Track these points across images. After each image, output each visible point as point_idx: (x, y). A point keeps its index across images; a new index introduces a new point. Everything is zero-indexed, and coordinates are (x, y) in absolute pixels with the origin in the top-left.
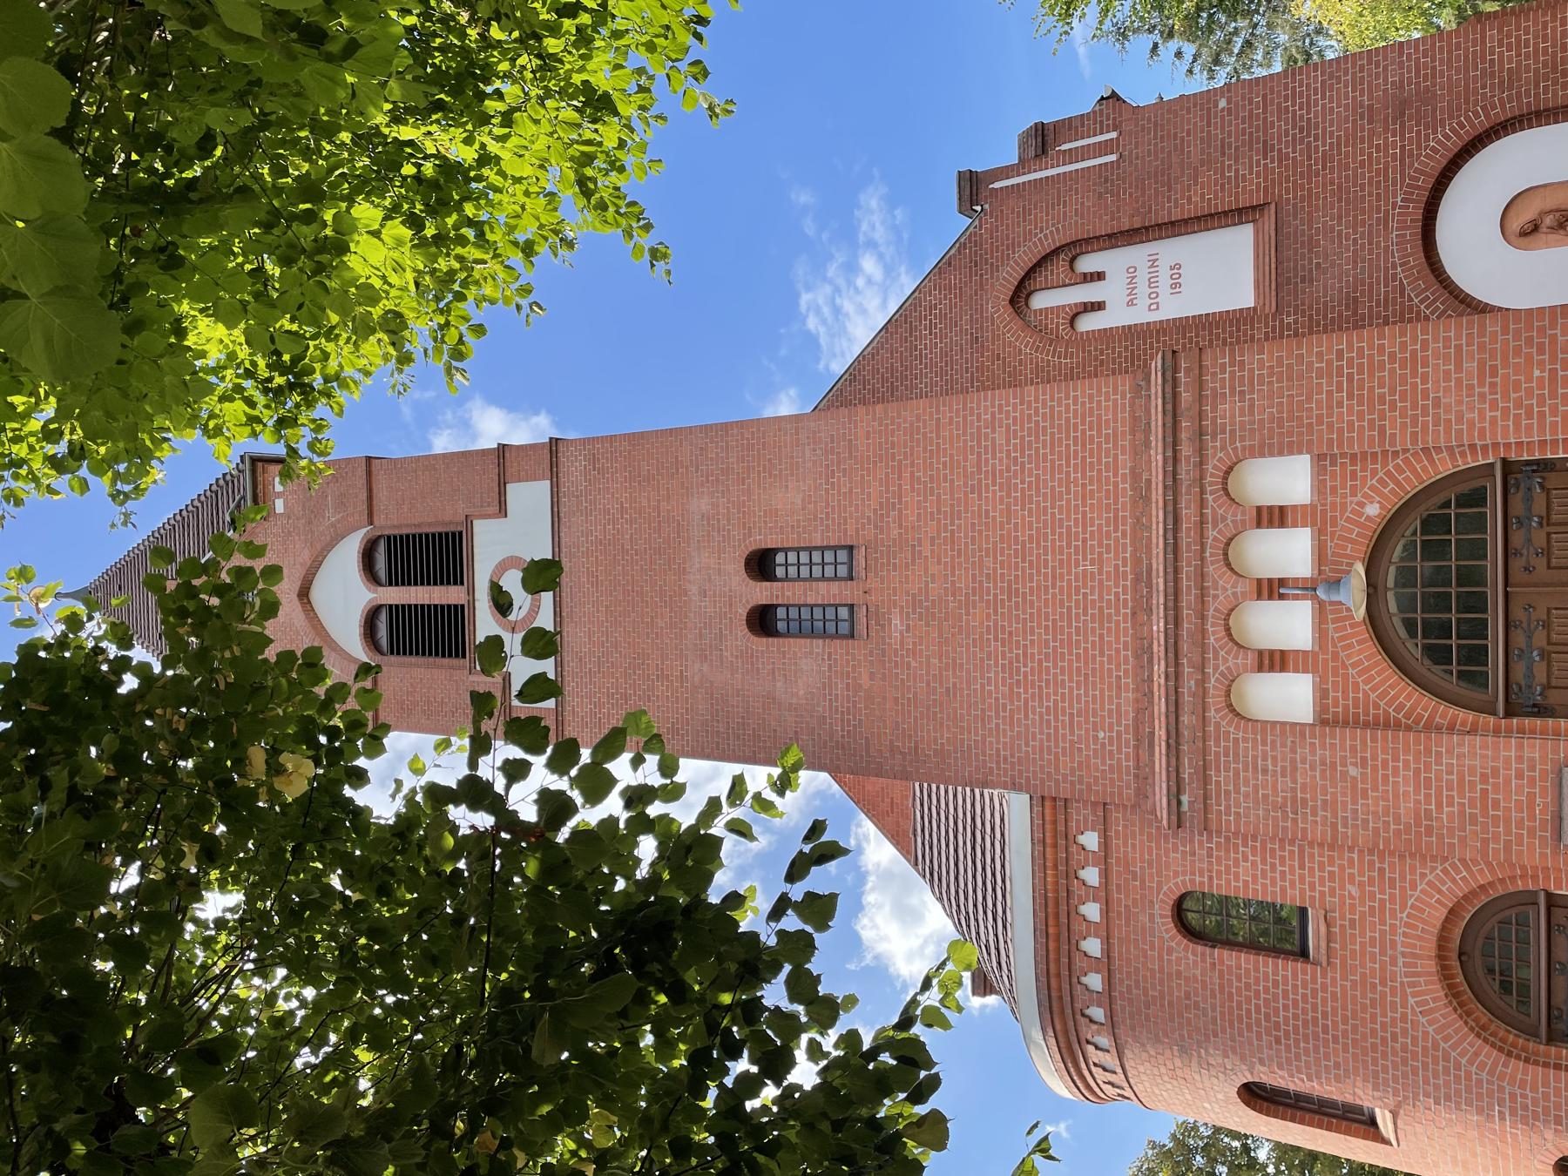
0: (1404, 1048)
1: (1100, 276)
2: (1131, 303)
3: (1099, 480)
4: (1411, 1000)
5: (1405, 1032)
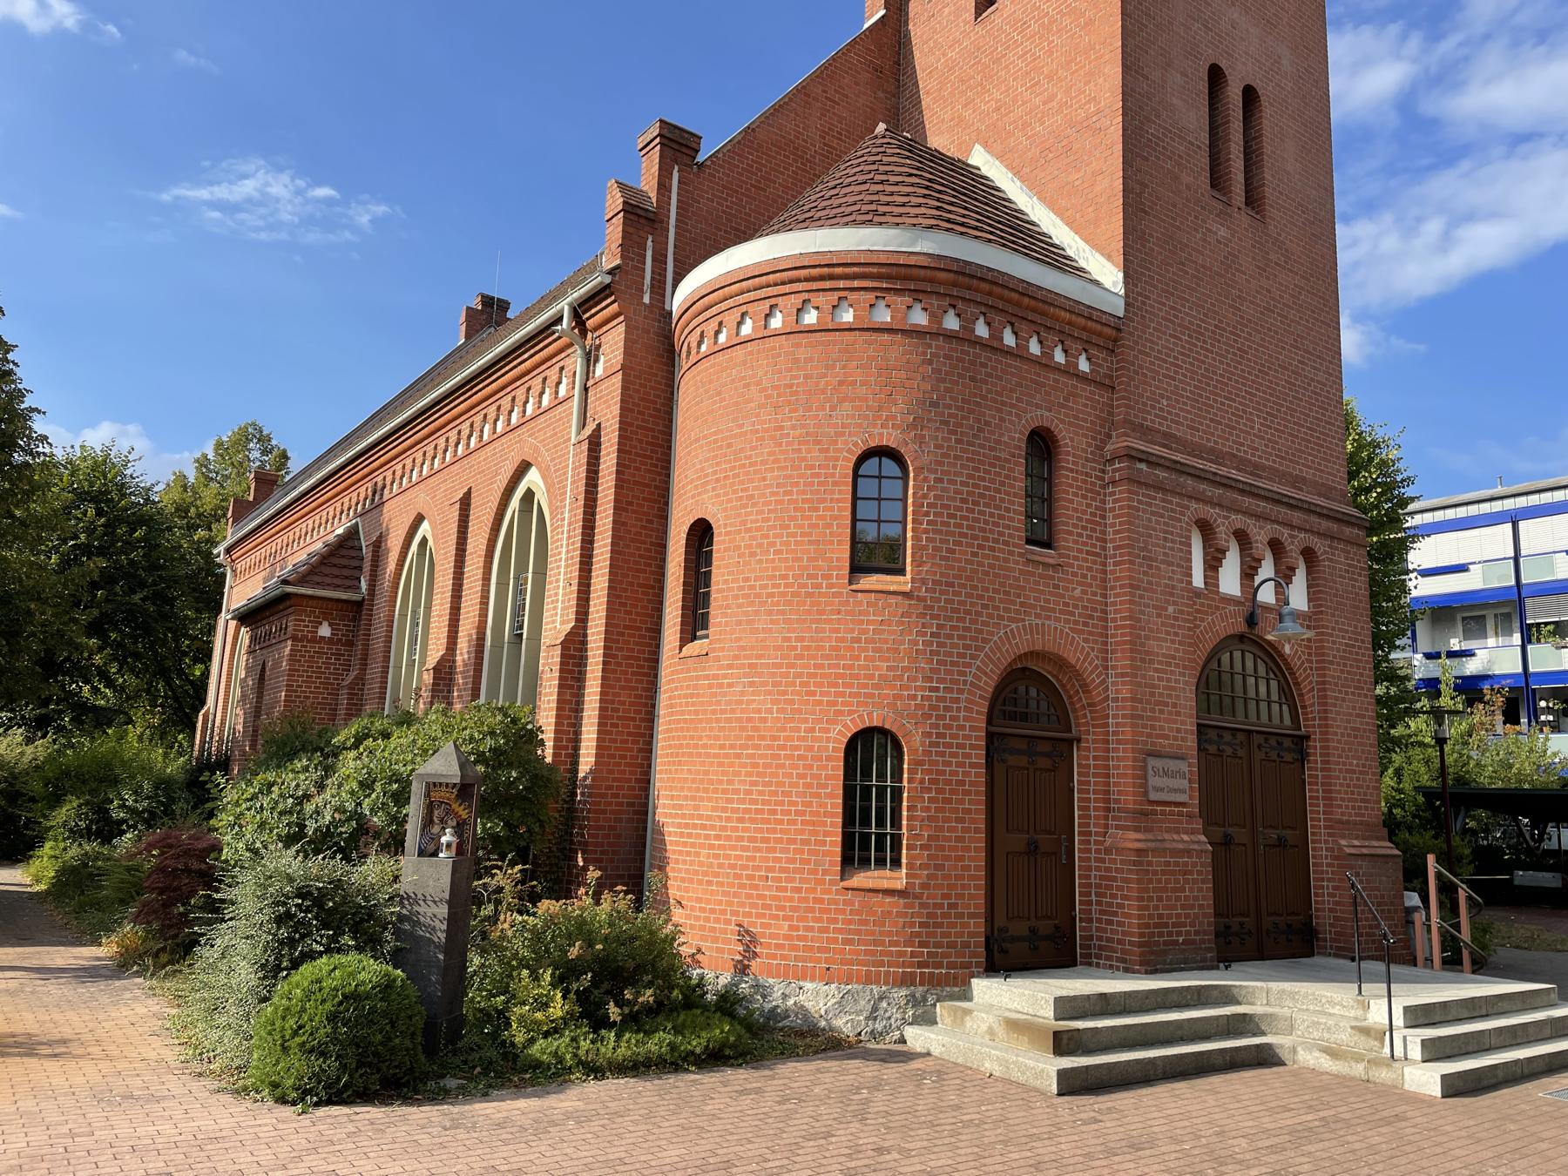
0: (978, 614)
5: (990, 616)
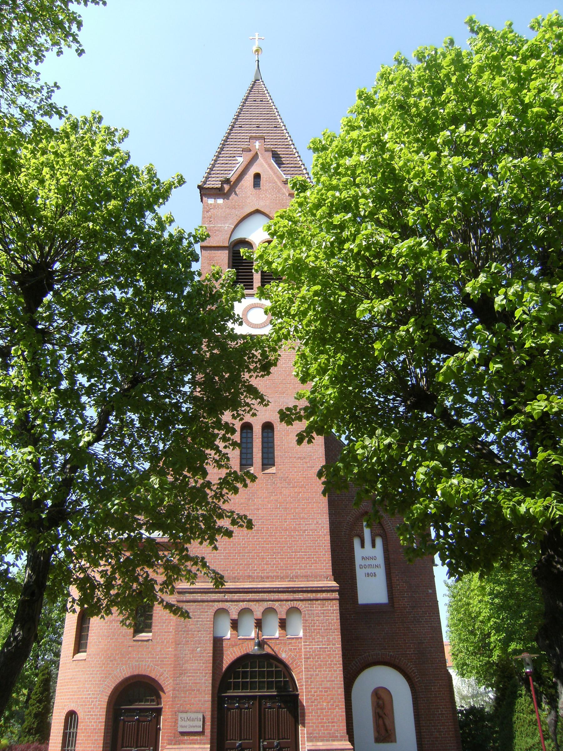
0: (108, 664)
1: (374, 546)
2: (363, 558)
3: (296, 564)
4: (124, 667)
